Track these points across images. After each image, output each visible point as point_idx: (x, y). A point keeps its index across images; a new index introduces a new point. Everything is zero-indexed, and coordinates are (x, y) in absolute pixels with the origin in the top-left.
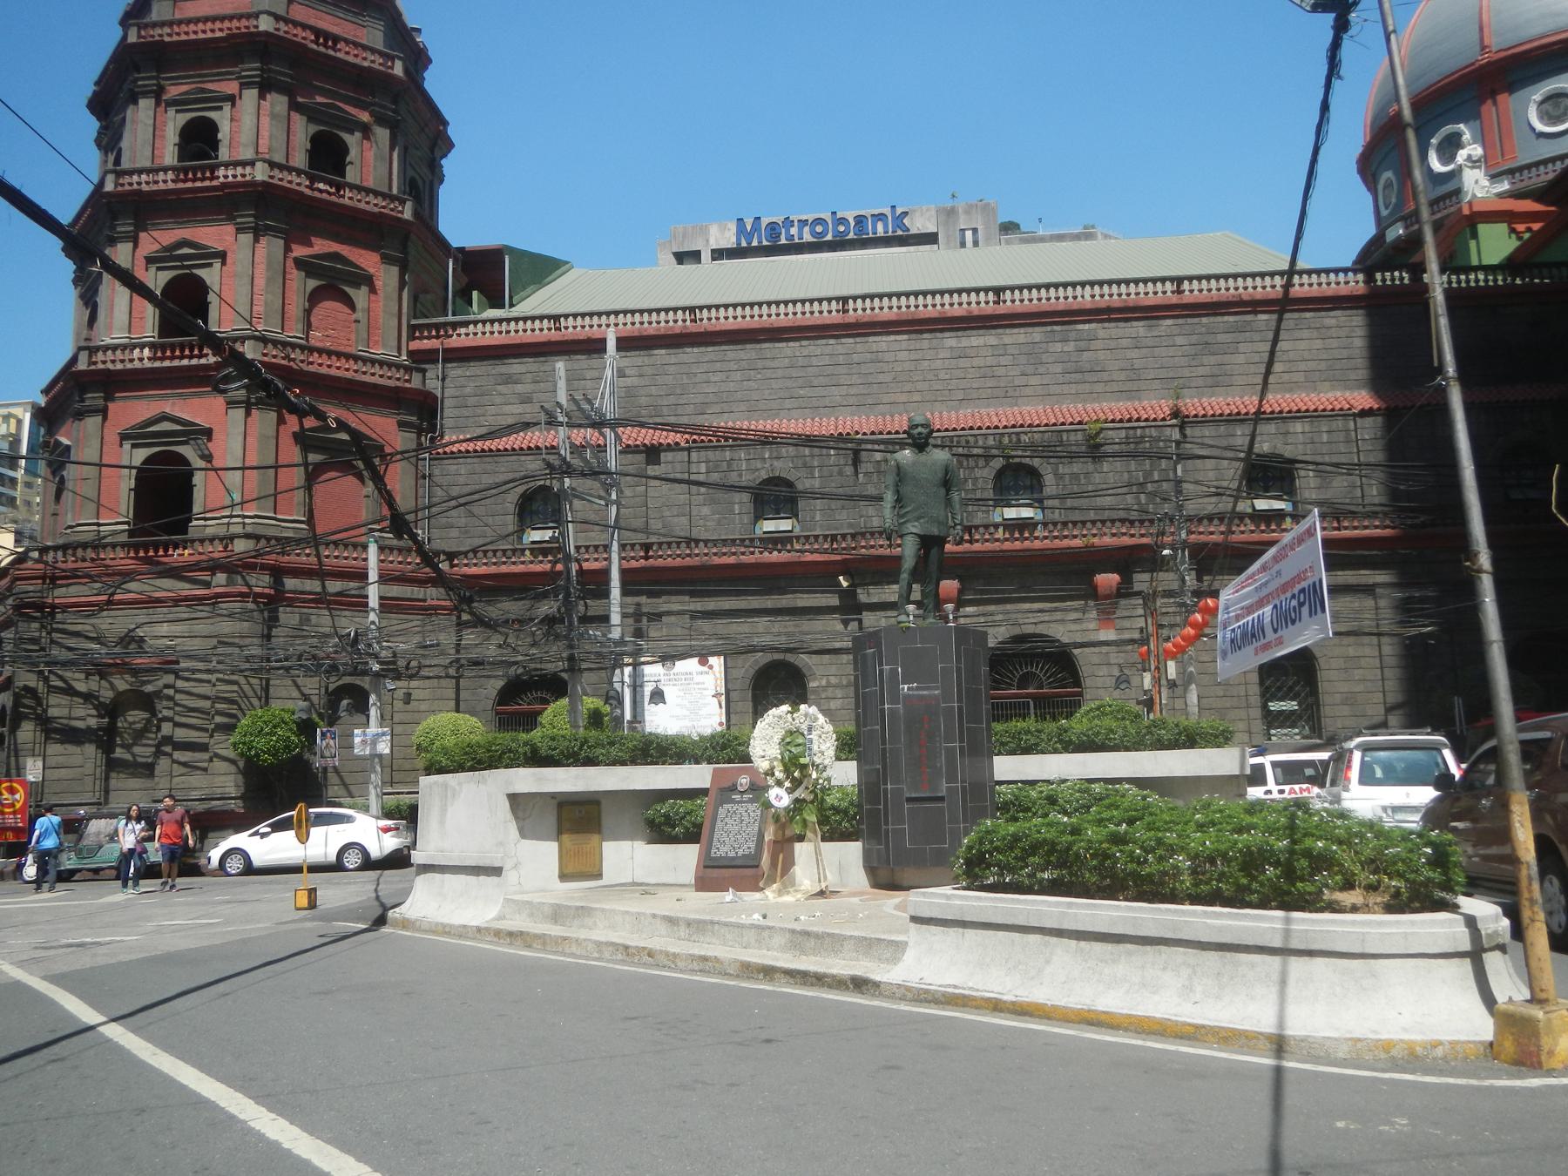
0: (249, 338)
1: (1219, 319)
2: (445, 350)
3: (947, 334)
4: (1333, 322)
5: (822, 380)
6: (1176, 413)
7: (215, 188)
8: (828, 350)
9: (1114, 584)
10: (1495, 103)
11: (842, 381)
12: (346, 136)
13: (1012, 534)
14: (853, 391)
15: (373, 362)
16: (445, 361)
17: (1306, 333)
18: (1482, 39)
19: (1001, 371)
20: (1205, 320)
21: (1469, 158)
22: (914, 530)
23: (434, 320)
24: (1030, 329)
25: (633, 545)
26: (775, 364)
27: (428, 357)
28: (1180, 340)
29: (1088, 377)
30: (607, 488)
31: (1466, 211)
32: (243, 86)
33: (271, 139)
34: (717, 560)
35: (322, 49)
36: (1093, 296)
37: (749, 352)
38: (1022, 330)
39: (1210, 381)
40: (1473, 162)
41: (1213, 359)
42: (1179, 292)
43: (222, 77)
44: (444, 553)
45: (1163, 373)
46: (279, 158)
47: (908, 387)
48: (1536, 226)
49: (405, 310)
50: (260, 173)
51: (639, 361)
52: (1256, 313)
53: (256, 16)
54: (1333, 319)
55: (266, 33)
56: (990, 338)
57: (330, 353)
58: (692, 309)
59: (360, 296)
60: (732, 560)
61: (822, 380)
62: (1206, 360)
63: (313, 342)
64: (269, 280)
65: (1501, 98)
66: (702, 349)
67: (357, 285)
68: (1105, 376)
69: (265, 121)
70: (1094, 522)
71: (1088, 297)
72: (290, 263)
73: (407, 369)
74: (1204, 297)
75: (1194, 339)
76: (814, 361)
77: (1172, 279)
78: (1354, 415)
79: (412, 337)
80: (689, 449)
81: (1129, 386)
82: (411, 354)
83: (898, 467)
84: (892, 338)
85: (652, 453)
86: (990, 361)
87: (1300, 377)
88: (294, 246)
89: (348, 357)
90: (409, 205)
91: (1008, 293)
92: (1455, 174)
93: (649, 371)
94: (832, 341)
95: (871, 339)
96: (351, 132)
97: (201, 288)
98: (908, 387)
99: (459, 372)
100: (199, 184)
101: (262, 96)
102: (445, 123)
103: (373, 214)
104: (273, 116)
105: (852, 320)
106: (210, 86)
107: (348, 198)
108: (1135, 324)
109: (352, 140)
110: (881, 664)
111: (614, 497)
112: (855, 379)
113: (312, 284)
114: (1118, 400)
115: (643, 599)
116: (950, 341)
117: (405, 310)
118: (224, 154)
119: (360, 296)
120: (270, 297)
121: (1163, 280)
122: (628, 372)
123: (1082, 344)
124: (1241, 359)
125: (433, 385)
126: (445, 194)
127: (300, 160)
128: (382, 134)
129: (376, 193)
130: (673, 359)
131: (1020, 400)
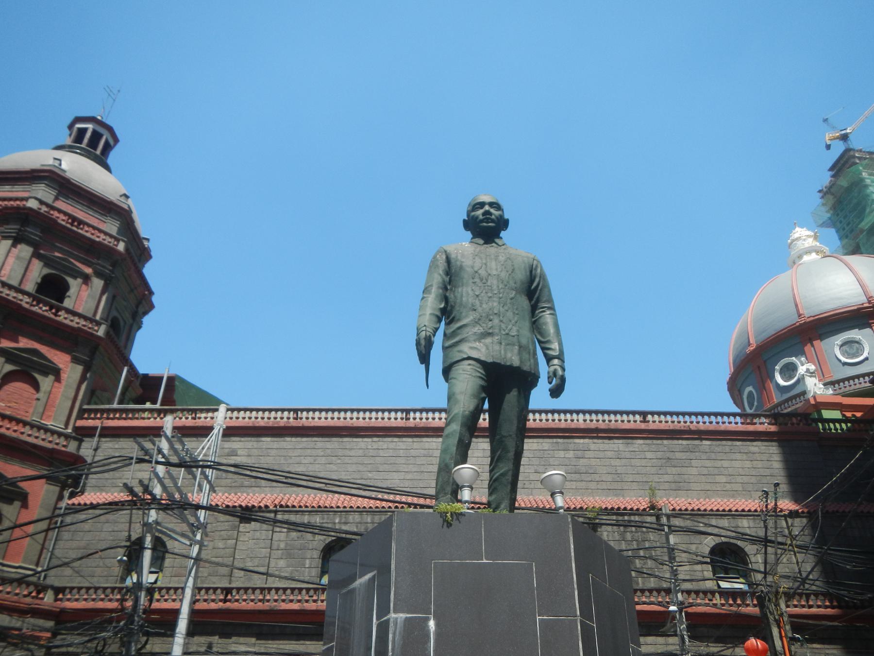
1: (676, 442)
2: (103, 428)
4: (755, 449)
5: (387, 467)
6: (652, 507)
8: (392, 446)
10: (813, 346)
11: (401, 469)
12: (70, 280)
14: (409, 476)
15: (40, 428)
16: (101, 436)
17: (738, 456)
18: (798, 311)
20: (665, 442)
21: (808, 370)
22: (475, 354)
23: (102, 407)
24: (541, 440)
25: (215, 589)
26: (352, 453)
27: (89, 432)
28: (649, 455)
29: (584, 477)
30: (194, 528)
31: (813, 402)
34: (284, 606)
36: (585, 421)
37: (334, 443)
38: (535, 440)
40: (812, 374)
41: (674, 470)
42: (645, 421)
45: (638, 478)
46: (14, 283)
48: (859, 414)
49: (80, 397)
52: (701, 439)
53: (26, 199)
54: (756, 447)
55: (30, 209)
58: (296, 411)
60: (295, 606)
61: (387, 467)
62: (669, 470)
65: (816, 343)
66: (299, 439)
67: (45, 374)
68: (597, 477)
69: (11, 260)
71: (581, 421)
73: (67, 437)
74: (663, 426)
75: (659, 455)
76: (381, 453)
77: (641, 413)
78: (785, 516)
79: (80, 417)
80: (276, 512)
81: (615, 486)
82: (76, 429)
83: (448, 260)
85: (246, 514)
87: (739, 487)
89: (18, 421)
92: (801, 380)
93: (256, 452)
94: (396, 439)
95: (425, 439)
96: (75, 278)
99: (110, 445)
101: (14, 245)
102: (151, 293)
103: (72, 328)
104: (18, 258)
105: (413, 425)
108: (616, 441)
109: (74, 284)
110: (384, 610)
111: (198, 537)
112: (411, 468)
113: (9, 368)
114: (607, 496)
115: (215, 639)
117: (80, 397)
119: (46, 382)
121: (634, 413)
122: (239, 452)
123: (579, 453)
124: (694, 471)
125: (86, 451)
126: (141, 337)
127: (30, 286)
128: (98, 283)
129: (80, 316)
130: (275, 445)
131: (534, 491)
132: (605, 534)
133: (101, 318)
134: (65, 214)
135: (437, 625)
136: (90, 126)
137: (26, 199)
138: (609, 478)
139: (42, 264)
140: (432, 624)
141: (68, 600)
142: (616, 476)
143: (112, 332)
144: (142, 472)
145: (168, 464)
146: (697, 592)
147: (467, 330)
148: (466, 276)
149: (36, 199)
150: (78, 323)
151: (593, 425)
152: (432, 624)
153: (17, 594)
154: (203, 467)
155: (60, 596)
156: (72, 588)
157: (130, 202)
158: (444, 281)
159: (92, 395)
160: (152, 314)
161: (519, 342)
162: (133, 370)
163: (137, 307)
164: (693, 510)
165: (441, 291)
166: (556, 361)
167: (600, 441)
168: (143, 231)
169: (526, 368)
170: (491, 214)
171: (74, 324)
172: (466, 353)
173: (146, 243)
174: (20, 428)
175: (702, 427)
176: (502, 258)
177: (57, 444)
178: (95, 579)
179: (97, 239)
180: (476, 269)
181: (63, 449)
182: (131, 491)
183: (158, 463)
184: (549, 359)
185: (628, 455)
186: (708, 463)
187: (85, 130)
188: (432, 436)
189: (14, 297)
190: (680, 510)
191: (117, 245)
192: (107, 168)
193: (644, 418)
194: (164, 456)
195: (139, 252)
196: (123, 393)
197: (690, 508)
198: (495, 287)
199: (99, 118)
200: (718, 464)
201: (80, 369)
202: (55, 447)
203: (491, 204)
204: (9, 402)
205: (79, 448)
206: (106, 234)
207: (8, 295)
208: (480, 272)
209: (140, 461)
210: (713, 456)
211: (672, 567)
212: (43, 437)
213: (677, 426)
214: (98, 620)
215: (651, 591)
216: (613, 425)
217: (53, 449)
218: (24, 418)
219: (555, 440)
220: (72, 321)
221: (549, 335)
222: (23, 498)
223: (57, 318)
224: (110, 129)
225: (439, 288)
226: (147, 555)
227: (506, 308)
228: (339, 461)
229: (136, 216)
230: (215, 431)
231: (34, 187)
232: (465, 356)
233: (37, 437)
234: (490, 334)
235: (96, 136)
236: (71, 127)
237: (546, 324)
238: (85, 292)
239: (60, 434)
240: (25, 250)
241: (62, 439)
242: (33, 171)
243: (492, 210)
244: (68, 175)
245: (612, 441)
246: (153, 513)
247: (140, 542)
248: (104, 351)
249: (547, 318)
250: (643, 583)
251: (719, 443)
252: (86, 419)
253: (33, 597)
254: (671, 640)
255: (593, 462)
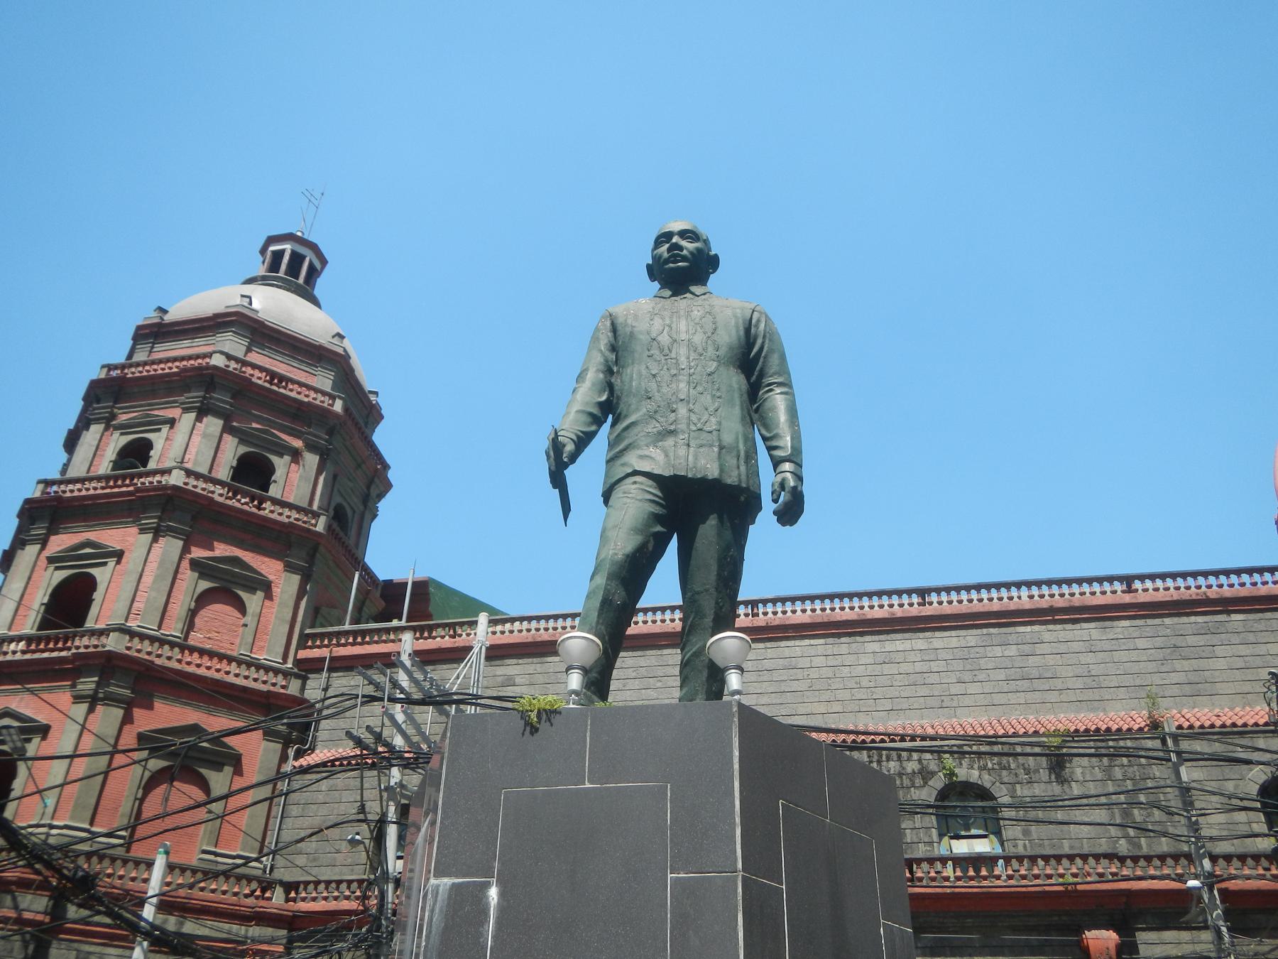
0: (114, 630)
1: (1185, 619)
2: (333, 659)
3: (868, 638)
6: (1155, 725)
7: (129, 493)
9: (1112, 946)
12: (275, 459)
13: (965, 871)
15: (249, 665)
16: (331, 670)
19: (934, 678)
20: (1167, 621)
23: (330, 629)
28: (1141, 643)
29: (1037, 684)
32: (186, 410)
33: (199, 459)
35: (267, 385)
36: (1031, 597)
38: (953, 633)
39: (1188, 689)
41: (1186, 664)
42: (1130, 590)
43: (169, 405)
44: (282, 883)
45: (1127, 680)
46: (203, 470)
47: (827, 696)
50: (177, 479)
51: (530, 669)
52: (1229, 613)
53: (210, 355)
55: (215, 367)
56: (918, 642)
57: (202, 652)
59: (253, 601)
62: (1178, 665)
63: (191, 642)
64: (158, 578)
67: (252, 590)
68: (1058, 684)
69: (196, 439)
70: (1071, 858)
72: (185, 564)
73: (286, 674)
74: (1161, 596)
75: (1159, 642)
77: (1121, 579)
82: (298, 662)
84: (807, 642)
86: (919, 667)
88: (193, 549)
89: (222, 657)
90: (323, 519)
91: (934, 594)
95: (783, 644)
96: (281, 455)
97: (91, 583)
98: (827, 696)
100: (116, 490)
101: (199, 419)
102: (386, 467)
103: (282, 524)
104: (205, 436)
105: (763, 624)
106: (156, 413)
107: (268, 510)
108: (1085, 625)
109: (280, 464)
113: (205, 585)
116: (872, 645)
118: (152, 465)
119: (253, 601)
120: (154, 594)
121: (1111, 579)
122: (518, 680)
123: (1027, 649)
124: (1221, 664)
125: (313, 691)
127: (223, 473)
128: (312, 460)
131: (959, 711)
132: (1079, 771)
133: (319, 508)
134: (261, 369)
135: (502, 895)
136: (287, 247)
137: (210, 355)
138: (1079, 683)
139: (236, 440)
140: (493, 893)
141: (304, 899)
142: (1089, 680)
143: (335, 525)
144: (372, 715)
145: (409, 701)
146: (1242, 858)
147: (635, 430)
148: (638, 348)
149: (222, 353)
150: (289, 517)
151: (1044, 604)
152: (493, 893)
153: (236, 894)
154: (458, 702)
155: (293, 894)
156: (307, 883)
157: (346, 343)
158: (607, 361)
159: (315, 615)
160: (389, 496)
161: (720, 440)
162: (367, 573)
163: (368, 488)
164: (1223, 726)
165: (601, 376)
166: (787, 466)
167: (1059, 627)
168: (368, 380)
169: (731, 479)
170: (681, 248)
171: (284, 519)
172: (632, 466)
173: (372, 398)
174: (224, 666)
175: (1227, 592)
176: (696, 314)
177: (274, 685)
178: (337, 869)
179: (306, 400)
180: (654, 335)
181: (282, 691)
182: (359, 742)
183: (393, 700)
184: (776, 463)
185: (1107, 646)
186: (1243, 650)
187: (283, 251)
188: (794, 638)
189: (204, 489)
190: (1202, 727)
191: (332, 405)
192: (315, 302)
193: (1129, 586)
194: (403, 691)
195: (364, 412)
196: (359, 608)
197: (1218, 723)
198: (683, 359)
199: (299, 234)
200: (1262, 649)
201: (296, 579)
202: (272, 688)
203: (683, 234)
204: (209, 631)
205: (303, 688)
206: (316, 390)
207: (195, 487)
208: (660, 338)
209: (372, 699)
210: (1251, 638)
211: (1189, 818)
212: (256, 676)
213: (1185, 595)
214: (333, 925)
215: (1162, 858)
216: (1077, 601)
217: (269, 691)
218: (229, 652)
219: (985, 631)
220: (280, 514)
221: (778, 425)
222: (235, 761)
223: (261, 513)
224: (314, 247)
225: (598, 371)
226: (392, 832)
227: (700, 389)
228: (659, 684)
229: (356, 362)
230: (476, 650)
231: (219, 337)
232: (630, 471)
233: (246, 678)
234: (672, 433)
235: (297, 259)
236: (263, 251)
237: (774, 409)
238: (296, 473)
239: (277, 672)
240: (213, 424)
241: (280, 677)
242: (216, 316)
243: (684, 243)
244: (262, 316)
245: (1078, 626)
246: (395, 772)
247: (384, 815)
248: (328, 551)
249: (778, 401)
250: (1149, 846)
251: (1260, 615)
252: (310, 648)
253: (257, 898)
254: (1207, 936)
255: (1050, 660)
